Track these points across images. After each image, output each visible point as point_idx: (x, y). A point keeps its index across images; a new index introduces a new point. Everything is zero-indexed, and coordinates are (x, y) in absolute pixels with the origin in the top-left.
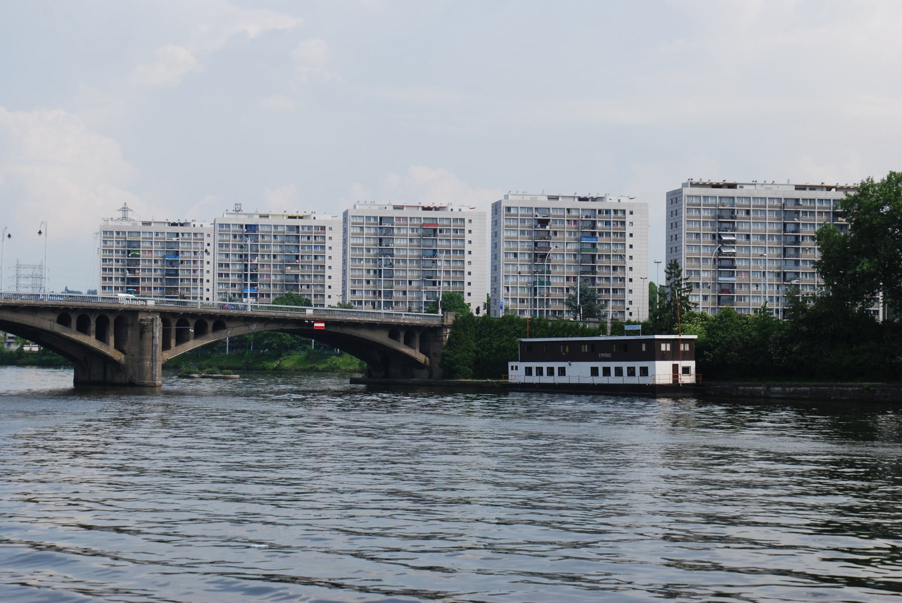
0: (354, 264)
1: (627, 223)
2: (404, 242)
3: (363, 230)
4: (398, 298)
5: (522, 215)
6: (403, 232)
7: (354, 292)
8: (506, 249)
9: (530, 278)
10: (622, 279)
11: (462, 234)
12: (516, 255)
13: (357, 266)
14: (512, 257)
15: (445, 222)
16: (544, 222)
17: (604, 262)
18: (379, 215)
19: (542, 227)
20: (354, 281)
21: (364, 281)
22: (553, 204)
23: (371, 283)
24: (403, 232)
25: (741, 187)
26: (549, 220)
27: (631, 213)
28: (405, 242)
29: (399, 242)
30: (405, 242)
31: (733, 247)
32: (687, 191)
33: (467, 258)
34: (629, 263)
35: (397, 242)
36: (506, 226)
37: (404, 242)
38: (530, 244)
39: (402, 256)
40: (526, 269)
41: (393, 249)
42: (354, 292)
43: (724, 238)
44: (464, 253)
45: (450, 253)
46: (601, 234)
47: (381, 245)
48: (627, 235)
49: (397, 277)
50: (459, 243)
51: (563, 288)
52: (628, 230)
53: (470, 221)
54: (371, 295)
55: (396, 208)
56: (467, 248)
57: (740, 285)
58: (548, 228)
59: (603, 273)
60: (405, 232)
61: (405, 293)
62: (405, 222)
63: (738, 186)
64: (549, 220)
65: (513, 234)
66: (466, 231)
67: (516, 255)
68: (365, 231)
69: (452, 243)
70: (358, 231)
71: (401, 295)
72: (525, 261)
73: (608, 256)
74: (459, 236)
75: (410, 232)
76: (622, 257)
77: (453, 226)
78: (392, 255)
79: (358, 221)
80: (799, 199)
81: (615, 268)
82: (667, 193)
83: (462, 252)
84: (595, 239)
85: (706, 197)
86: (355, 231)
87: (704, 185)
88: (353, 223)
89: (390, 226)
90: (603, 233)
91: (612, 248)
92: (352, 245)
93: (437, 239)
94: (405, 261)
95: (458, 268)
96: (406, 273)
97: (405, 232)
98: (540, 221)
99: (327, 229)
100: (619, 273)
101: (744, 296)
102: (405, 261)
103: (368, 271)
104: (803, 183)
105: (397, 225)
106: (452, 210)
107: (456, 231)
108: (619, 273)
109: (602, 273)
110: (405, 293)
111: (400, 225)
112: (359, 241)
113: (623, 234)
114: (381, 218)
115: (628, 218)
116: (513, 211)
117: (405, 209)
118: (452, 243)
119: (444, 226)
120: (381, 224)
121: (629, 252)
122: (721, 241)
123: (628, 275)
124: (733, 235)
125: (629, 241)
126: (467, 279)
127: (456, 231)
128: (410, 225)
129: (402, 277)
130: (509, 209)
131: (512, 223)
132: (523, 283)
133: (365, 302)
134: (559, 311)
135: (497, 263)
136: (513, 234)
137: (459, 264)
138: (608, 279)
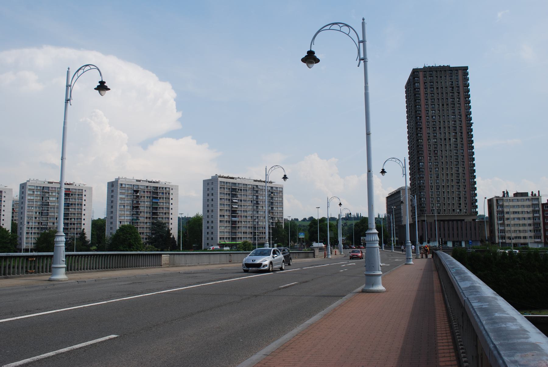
0: (29, 209)
1: (171, 194)
2: (54, 199)
3: (34, 193)
4: (50, 226)
5: (127, 188)
6: (54, 194)
7: (28, 223)
8: (120, 203)
9: (130, 217)
10: (168, 218)
11: (81, 196)
12: (124, 206)
13: (30, 210)
14: (123, 207)
15: (74, 191)
16: (137, 192)
17: (161, 211)
18: (42, 186)
19: (136, 194)
20: (28, 217)
21: (34, 218)
22: (138, 183)
23: (37, 218)
24: (54, 194)
25: (236, 179)
26: (138, 191)
27: (172, 189)
28: (55, 199)
29: (51, 199)
30: (55, 199)
31: (236, 205)
32: (220, 179)
33: (84, 207)
34: (171, 211)
35: (51, 199)
36: (120, 193)
37: (54, 199)
38: (131, 201)
39: (53, 206)
40: (128, 213)
41: (49, 202)
42: (28, 223)
43: (234, 201)
44: (82, 205)
45: (76, 205)
46: (160, 198)
47: (42, 200)
48: (170, 199)
49: (51, 216)
50: (80, 201)
51: (144, 222)
52: (171, 197)
53: (85, 191)
54: (37, 224)
55: (49, 183)
56: (84, 203)
57: (239, 222)
58: (138, 194)
59: (161, 215)
60: (55, 194)
61: (54, 223)
62: (55, 190)
63: (235, 179)
64: (139, 191)
65: (123, 196)
66: (83, 195)
67: (124, 206)
68: (35, 193)
69: (77, 200)
70: (32, 193)
71: (52, 224)
72: (128, 209)
73: (163, 208)
74: (80, 197)
75: (57, 195)
76: (168, 208)
77: (78, 193)
78: (49, 205)
79: (32, 188)
80: (258, 185)
81: (165, 213)
82: (203, 180)
83: (81, 205)
84: (158, 200)
85: (227, 183)
86: (30, 193)
87: (225, 177)
88: (29, 189)
89: (48, 191)
90: (161, 197)
91: (165, 204)
92: (28, 199)
93: (69, 198)
94: (54, 208)
95: (79, 212)
96: (55, 214)
97: (55, 194)
98: (135, 191)
99: (3, 192)
100: (167, 216)
101: (240, 226)
102: (54, 208)
103: (36, 213)
104: (256, 179)
105: (51, 191)
106: (76, 185)
107: (79, 195)
108: (167, 216)
109: (160, 216)
110: (54, 223)
111: (52, 191)
112: (32, 198)
113: (169, 198)
114: (43, 187)
115: (171, 192)
116: (123, 186)
117: (53, 183)
118: (77, 200)
119: (73, 192)
120: (43, 190)
121: (171, 206)
122: (232, 202)
123: (171, 216)
124: (236, 200)
125: (171, 201)
126: (83, 217)
127: (79, 195)
128: (57, 191)
129: (52, 216)
130: (121, 184)
131: (123, 191)
132: (127, 220)
133: (34, 228)
134: (142, 233)
135: (112, 210)
136: (123, 196)
137: (80, 210)
138: (162, 218)
